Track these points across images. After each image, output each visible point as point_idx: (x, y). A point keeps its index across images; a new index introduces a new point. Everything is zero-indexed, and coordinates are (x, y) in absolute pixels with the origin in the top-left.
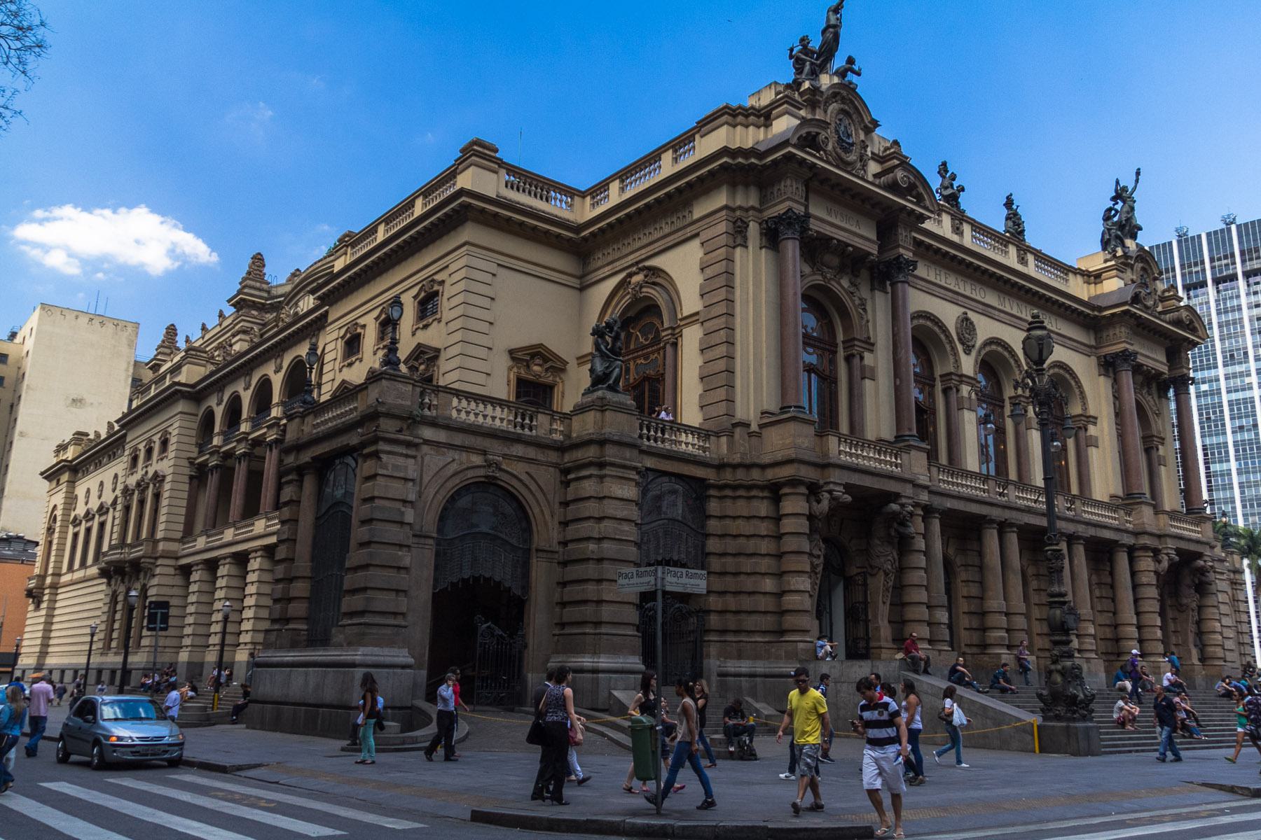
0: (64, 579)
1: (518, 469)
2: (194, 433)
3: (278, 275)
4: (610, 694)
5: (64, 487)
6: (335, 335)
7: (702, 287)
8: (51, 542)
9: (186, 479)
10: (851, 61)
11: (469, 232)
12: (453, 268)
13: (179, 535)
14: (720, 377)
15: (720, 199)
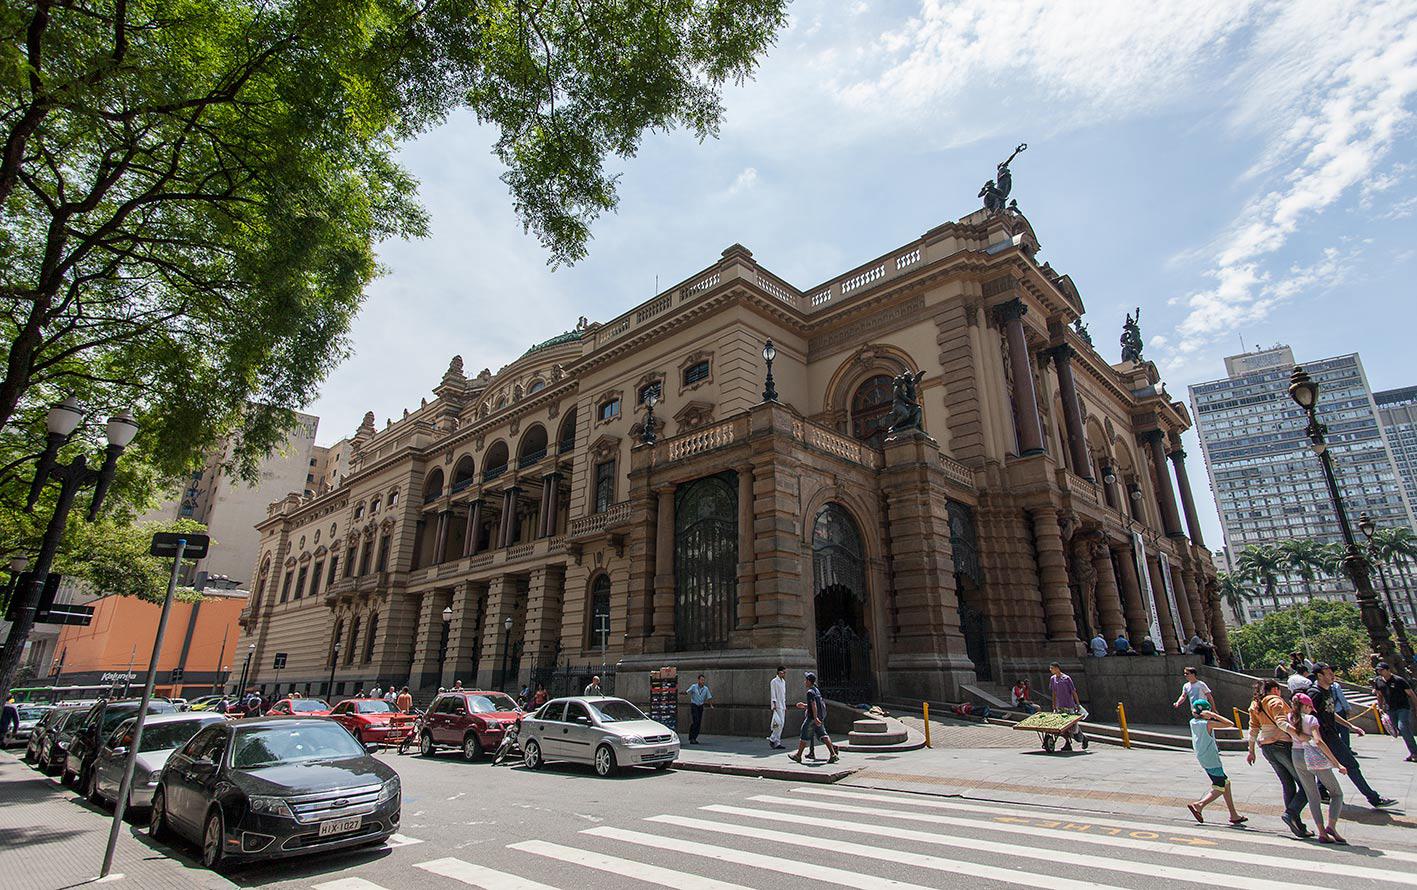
0: (276, 610)
1: (854, 491)
2: (420, 488)
3: (471, 372)
4: (960, 688)
5: (278, 536)
6: (588, 401)
7: (940, 357)
8: (263, 581)
9: (415, 524)
10: (1014, 203)
11: (739, 312)
12: (723, 342)
13: (409, 568)
14: (965, 426)
15: (954, 289)
